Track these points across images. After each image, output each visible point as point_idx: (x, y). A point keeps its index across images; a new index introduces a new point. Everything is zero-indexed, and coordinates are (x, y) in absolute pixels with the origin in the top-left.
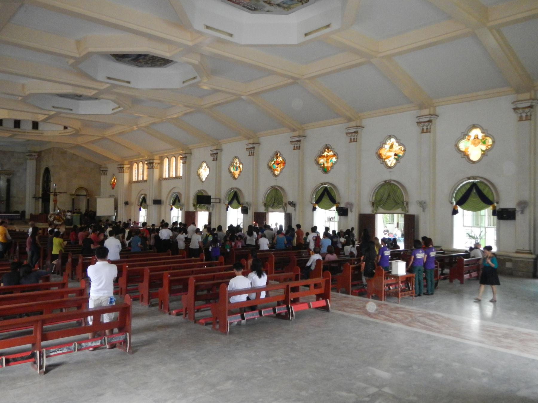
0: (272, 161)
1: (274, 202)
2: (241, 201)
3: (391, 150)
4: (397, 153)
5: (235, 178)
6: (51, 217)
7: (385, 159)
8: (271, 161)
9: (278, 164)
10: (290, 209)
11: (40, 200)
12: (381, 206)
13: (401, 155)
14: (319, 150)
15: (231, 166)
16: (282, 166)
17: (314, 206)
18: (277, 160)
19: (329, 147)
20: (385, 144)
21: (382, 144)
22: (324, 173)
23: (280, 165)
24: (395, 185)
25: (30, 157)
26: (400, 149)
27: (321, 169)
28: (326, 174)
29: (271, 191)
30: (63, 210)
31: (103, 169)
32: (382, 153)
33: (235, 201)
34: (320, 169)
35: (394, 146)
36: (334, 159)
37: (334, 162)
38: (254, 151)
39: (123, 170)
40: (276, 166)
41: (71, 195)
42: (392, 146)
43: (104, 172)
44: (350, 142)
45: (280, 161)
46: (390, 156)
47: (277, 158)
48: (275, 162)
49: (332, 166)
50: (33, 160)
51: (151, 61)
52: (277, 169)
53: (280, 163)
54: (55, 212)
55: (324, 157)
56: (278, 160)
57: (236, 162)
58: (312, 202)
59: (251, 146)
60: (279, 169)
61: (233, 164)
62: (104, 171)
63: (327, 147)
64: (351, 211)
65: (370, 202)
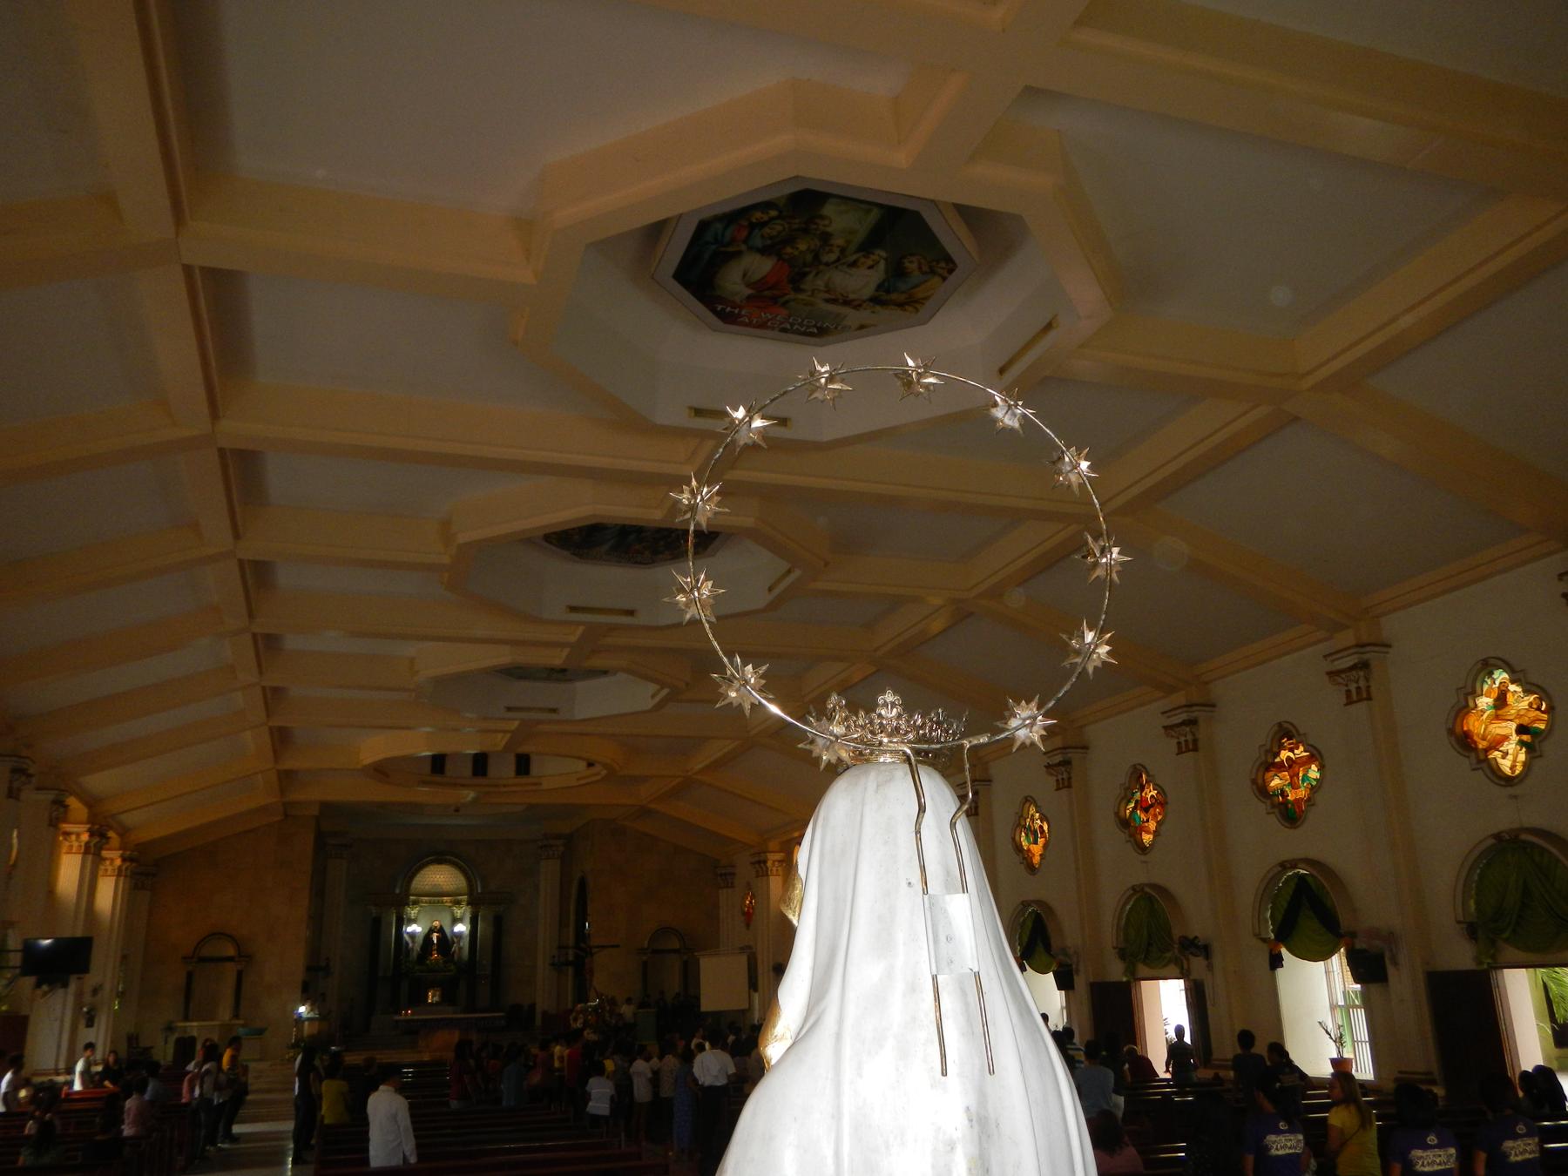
0: (1129, 802)
1: (1150, 944)
2: (1055, 943)
3: (1500, 712)
4: (1525, 721)
5: (1031, 868)
6: (576, 1020)
7: (1487, 751)
8: (1124, 801)
9: (1146, 810)
10: (1197, 963)
11: (570, 970)
12: (1506, 935)
13: (1542, 726)
14: (1261, 746)
15: (1017, 834)
16: (1160, 814)
17: (1271, 951)
18: (1143, 795)
19: (1291, 731)
20: (1474, 693)
21: (1462, 696)
22: (1286, 824)
23: (1152, 810)
24: (1543, 851)
26: (1535, 706)
27: (1276, 811)
28: (1295, 828)
29: (1135, 902)
30: (610, 997)
31: (723, 872)
32: (1471, 728)
33: (1040, 948)
34: (1273, 813)
35: (1510, 699)
36: (1314, 772)
37: (1314, 783)
38: (1069, 773)
39: (767, 868)
40: (1143, 817)
42: (1501, 701)
43: (723, 876)
44: (1346, 705)
45: (1152, 796)
46: (1506, 738)
47: (1142, 788)
48: (1137, 802)
49: (1309, 799)
51: (662, 543)
52: (1146, 824)
53: (1152, 806)
54: (589, 1004)
55: (1280, 767)
56: (1146, 794)
57: (1032, 816)
58: (1263, 936)
59: (1058, 759)
60: (1152, 825)
61: (1023, 823)
62: (725, 874)
63: (1286, 733)
64: (1395, 964)
65: (1459, 922)
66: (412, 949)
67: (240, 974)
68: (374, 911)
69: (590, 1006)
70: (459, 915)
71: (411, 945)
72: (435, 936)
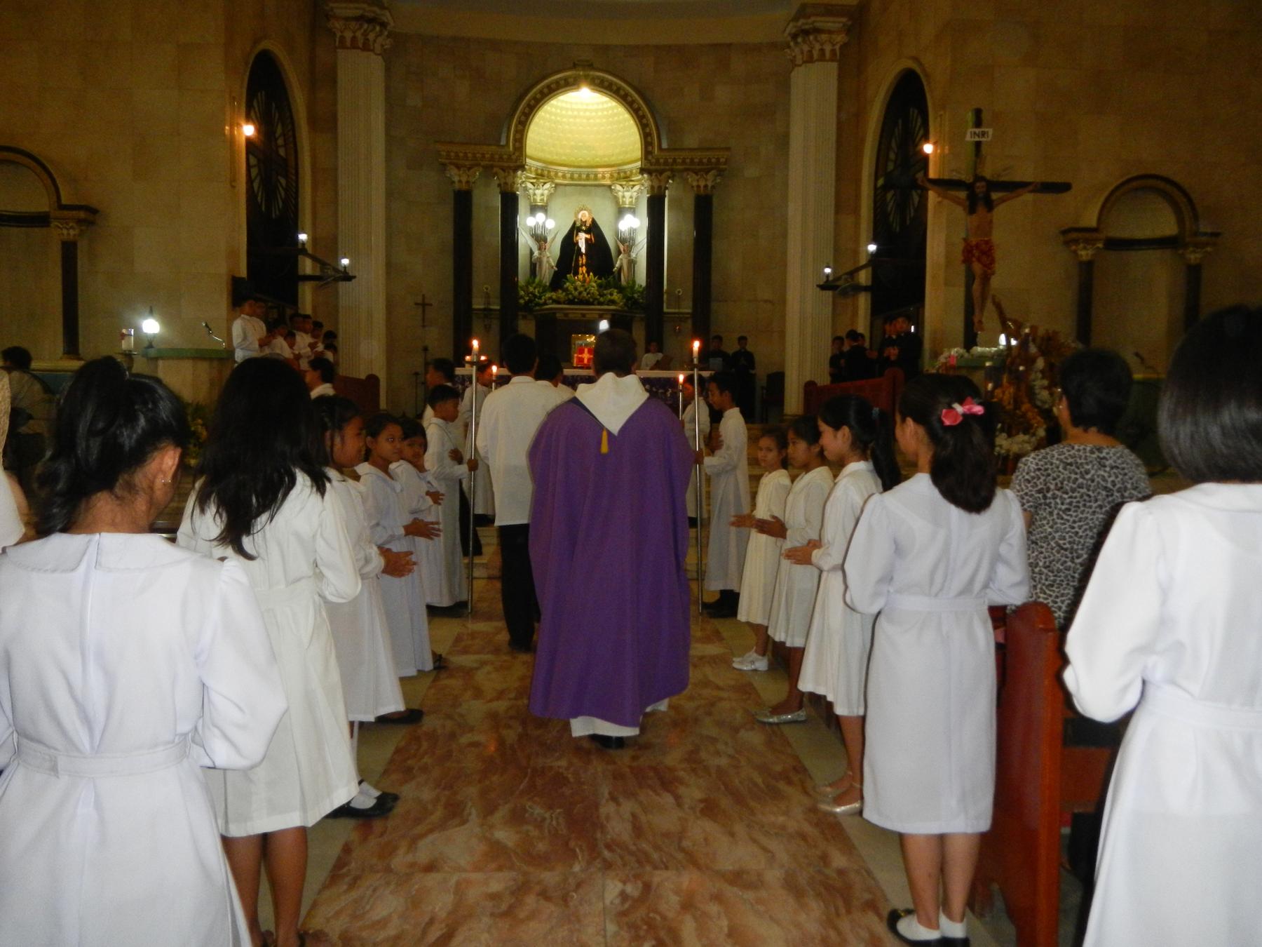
11: (863, 301)
25: (806, 48)
30: (1041, 332)
41: (1072, 235)
50: (822, 57)
54: (979, 349)
66: (540, 260)
67: (69, 252)
68: (456, 179)
69: (983, 357)
70: (628, 201)
71: (536, 253)
72: (582, 239)
